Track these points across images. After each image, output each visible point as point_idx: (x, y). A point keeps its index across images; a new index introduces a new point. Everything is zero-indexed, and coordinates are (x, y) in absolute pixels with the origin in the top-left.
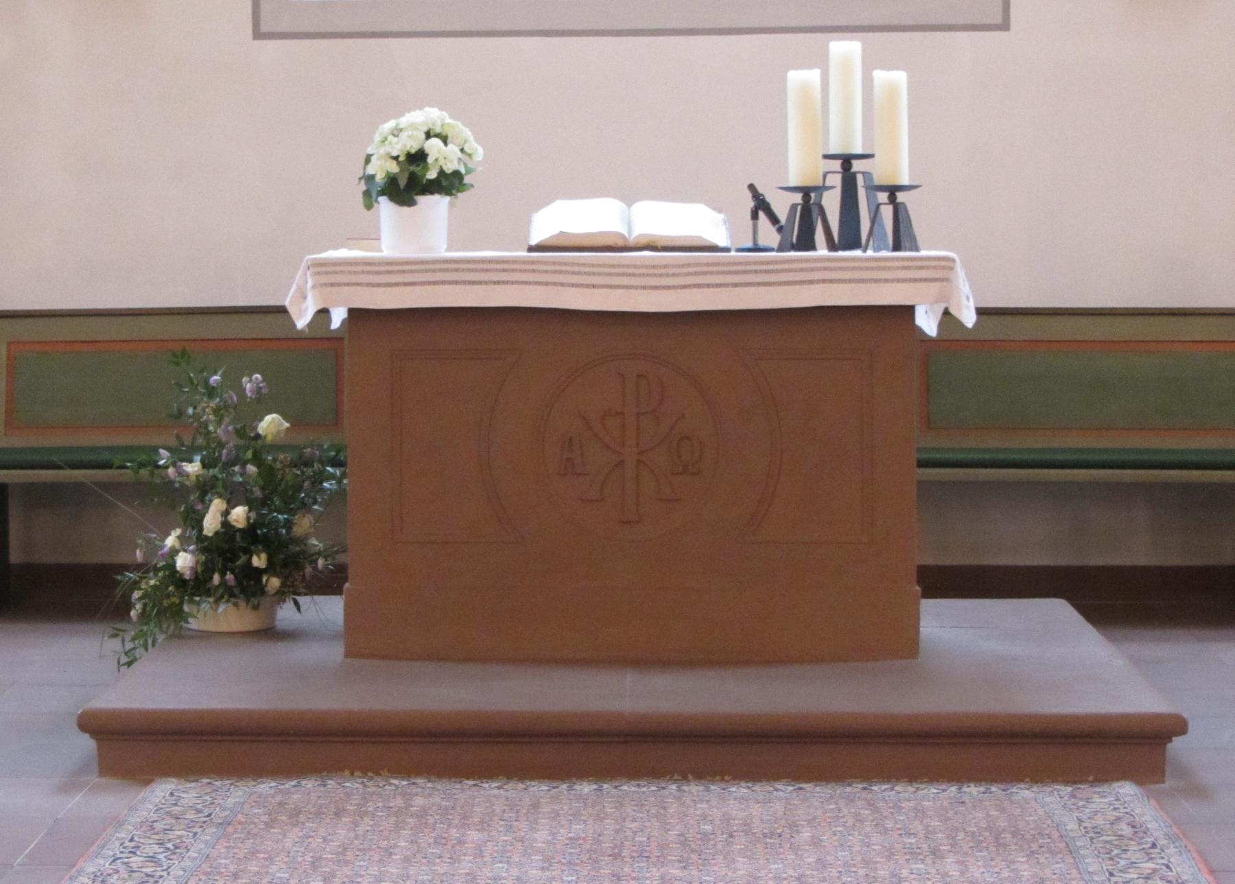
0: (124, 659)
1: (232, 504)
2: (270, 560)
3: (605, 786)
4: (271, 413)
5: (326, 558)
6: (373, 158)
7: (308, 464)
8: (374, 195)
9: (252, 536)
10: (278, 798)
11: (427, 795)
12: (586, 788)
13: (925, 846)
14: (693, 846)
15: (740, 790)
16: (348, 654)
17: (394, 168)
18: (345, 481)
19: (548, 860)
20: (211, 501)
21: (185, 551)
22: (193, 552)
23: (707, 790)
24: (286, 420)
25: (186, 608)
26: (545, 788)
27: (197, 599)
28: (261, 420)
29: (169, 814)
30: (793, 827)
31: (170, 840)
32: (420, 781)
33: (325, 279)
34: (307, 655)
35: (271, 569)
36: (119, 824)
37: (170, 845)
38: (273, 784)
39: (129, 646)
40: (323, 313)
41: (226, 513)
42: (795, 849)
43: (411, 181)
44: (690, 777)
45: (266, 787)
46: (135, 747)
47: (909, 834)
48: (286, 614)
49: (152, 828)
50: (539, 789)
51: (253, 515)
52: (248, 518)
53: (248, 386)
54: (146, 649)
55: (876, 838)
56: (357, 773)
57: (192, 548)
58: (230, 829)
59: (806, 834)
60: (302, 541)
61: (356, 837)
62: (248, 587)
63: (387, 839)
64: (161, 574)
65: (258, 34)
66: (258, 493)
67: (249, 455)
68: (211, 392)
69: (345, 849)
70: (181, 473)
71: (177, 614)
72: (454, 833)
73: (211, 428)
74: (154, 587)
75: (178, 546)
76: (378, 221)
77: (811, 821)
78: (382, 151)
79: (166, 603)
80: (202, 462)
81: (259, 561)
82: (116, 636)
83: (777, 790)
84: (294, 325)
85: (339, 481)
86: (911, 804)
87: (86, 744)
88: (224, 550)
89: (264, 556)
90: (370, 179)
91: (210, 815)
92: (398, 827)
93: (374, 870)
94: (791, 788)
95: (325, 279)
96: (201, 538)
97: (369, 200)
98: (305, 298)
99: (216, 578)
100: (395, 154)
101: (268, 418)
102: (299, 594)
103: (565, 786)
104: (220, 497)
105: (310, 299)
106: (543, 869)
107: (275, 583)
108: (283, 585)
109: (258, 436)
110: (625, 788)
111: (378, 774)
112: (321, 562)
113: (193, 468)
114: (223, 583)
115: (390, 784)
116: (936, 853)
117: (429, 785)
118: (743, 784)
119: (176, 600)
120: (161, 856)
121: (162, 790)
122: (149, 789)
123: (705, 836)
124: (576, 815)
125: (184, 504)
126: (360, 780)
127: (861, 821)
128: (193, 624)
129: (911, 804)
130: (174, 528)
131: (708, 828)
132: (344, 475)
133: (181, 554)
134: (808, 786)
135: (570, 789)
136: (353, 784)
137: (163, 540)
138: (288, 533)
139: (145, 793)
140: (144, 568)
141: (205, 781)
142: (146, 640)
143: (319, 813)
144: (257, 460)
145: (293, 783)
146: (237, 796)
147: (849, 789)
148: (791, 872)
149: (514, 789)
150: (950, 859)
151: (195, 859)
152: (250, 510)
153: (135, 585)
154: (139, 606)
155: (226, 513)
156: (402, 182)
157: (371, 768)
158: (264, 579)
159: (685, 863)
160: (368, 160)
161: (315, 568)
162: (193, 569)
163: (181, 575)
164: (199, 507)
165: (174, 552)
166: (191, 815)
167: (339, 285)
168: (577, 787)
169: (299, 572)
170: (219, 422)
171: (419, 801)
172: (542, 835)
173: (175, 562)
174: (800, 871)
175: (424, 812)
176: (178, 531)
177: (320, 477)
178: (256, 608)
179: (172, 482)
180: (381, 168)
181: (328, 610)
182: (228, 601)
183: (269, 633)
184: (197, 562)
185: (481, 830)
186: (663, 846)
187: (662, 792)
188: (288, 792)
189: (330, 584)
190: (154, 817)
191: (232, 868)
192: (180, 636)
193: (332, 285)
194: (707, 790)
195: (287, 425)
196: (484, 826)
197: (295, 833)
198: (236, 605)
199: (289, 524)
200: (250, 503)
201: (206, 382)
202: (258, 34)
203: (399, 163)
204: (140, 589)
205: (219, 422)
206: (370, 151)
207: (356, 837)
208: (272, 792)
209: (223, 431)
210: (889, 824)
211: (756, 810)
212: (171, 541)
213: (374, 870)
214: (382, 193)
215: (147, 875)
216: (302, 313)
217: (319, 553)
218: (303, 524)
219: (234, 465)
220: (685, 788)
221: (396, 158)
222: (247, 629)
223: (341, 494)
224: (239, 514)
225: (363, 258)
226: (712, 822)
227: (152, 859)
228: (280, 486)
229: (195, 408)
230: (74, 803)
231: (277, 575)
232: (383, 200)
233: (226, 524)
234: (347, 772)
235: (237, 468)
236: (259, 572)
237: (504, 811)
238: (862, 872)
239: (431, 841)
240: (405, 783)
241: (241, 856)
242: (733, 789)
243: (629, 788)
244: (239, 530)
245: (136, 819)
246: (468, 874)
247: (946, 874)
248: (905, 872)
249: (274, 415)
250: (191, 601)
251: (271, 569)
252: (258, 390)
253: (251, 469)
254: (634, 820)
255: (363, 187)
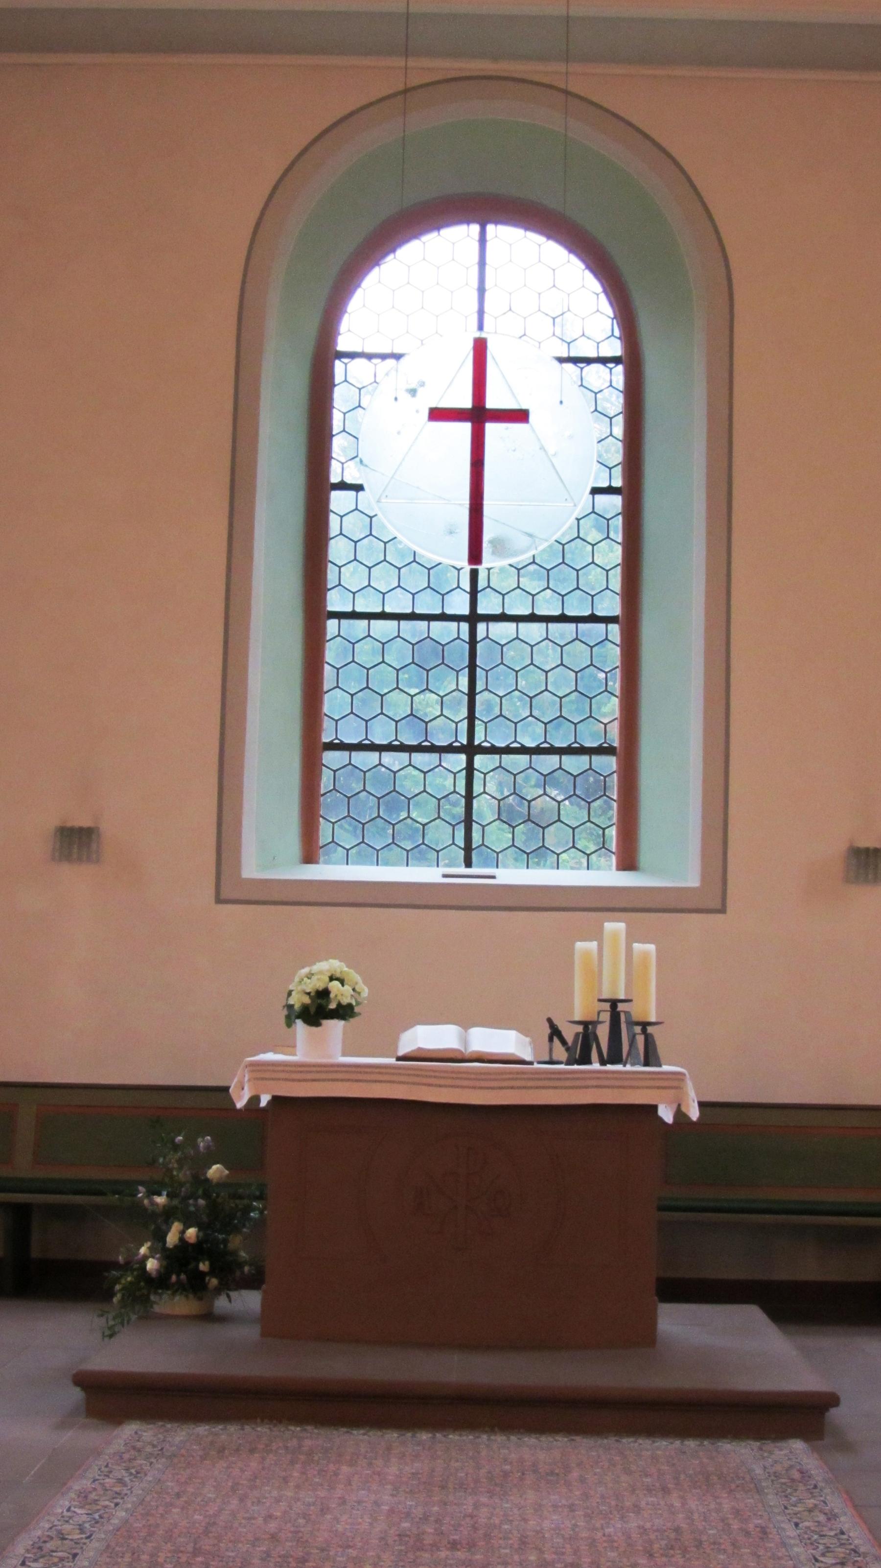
0: (107, 1332)
1: (187, 1227)
2: (211, 1265)
3: (438, 1435)
4: (218, 1163)
5: (250, 1265)
6: (293, 993)
7: (241, 1197)
8: (293, 1017)
9: (199, 1249)
10: (210, 1438)
11: (314, 1438)
12: (424, 1436)
13: (658, 1485)
14: (497, 1481)
15: (531, 1440)
16: (263, 1335)
17: (307, 1000)
18: (266, 1212)
19: (396, 1489)
20: (173, 1223)
21: (153, 1257)
22: (158, 1259)
23: (509, 1439)
24: (227, 1169)
25: (152, 1298)
26: (396, 1435)
27: (160, 1291)
28: (210, 1168)
29: (134, 1448)
30: (567, 1469)
31: (133, 1467)
32: (309, 1428)
33: (259, 1075)
34: (234, 1335)
35: (212, 1272)
36: (97, 1453)
37: (133, 1471)
38: (207, 1427)
39: (111, 1323)
40: (255, 1099)
41: (183, 1232)
42: (568, 1484)
43: (318, 1010)
44: (496, 1429)
45: (202, 1429)
46: (112, 1398)
47: (646, 1476)
48: (221, 1304)
49: (121, 1458)
50: (392, 1435)
51: (201, 1234)
52: (198, 1237)
53: (202, 1145)
54: (123, 1326)
55: (624, 1478)
56: (266, 1421)
57: (158, 1256)
58: (176, 1460)
59: (575, 1474)
60: (234, 1253)
61: (263, 1469)
62: (196, 1285)
63: (285, 1470)
64: (135, 1273)
65: (219, 900)
66: (205, 1219)
67: (200, 1192)
68: (176, 1147)
69: (256, 1478)
70: (153, 1203)
71: (145, 1301)
72: (332, 1467)
73: (175, 1173)
74: (131, 1283)
75: (148, 1253)
76: (295, 1034)
77: (580, 1464)
78: (300, 988)
79: (138, 1294)
80: (168, 1195)
81: (204, 1266)
82: (102, 1315)
83: (556, 1441)
84: (234, 1104)
85: (261, 1212)
86: (649, 1453)
87: (77, 1394)
88: (180, 1258)
89: (207, 1263)
90: (290, 1007)
91: (162, 1449)
92: (292, 1462)
93: (275, 1493)
94: (566, 1439)
95: (259, 1075)
96: (164, 1249)
97: (289, 1023)
98: (243, 1089)
99: (174, 1278)
100: (308, 991)
101: (215, 1167)
102: (230, 1290)
103: (409, 1435)
104: (179, 1220)
105: (246, 1088)
106: (392, 1495)
107: (214, 1282)
108: (220, 1283)
109: (207, 1180)
110: (451, 1436)
111: (280, 1422)
112: (246, 1269)
113: (161, 1200)
114: (179, 1281)
115: (288, 1430)
116: (665, 1490)
117: (316, 1431)
118: (534, 1436)
119: (145, 1292)
120: (127, 1479)
121: (129, 1429)
122: (120, 1428)
123: (506, 1475)
124: (417, 1456)
125: (155, 1224)
126: (267, 1426)
127: (614, 1465)
128: (157, 1309)
129: (649, 1453)
130: (146, 1241)
131: (508, 1467)
132: (265, 1208)
133: (150, 1259)
134: (578, 1439)
135: (413, 1436)
136: (263, 1429)
137: (139, 1249)
138: (225, 1246)
139: (117, 1431)
140: (127, 1266)
141: (160, 1423)
142: (123, 1319)
143: (238, 1450)
144: (206, 1195)
145: (220, 1427)
146: (181, 1435)
147: (605, 1441)
148: (564, 1502)
149: (374, 1435)
150: (675, 1495)
151: (150, 1481)
152: (199, 1230)
153: (117, 1280)
154: (119, 1296)
155: (183, 1232)
156: (313, 1010)
157: (276, 1418)
158: (207, 1278)
159: (491, 1494)
160: (290, 994)
161: (243, 1272)
162: (158, 1271)
163: (150, 1274)
164: (164, 1227)
165: (145, 1258)
166: (149, 1449)
167: (266, 1079)
168: (418, 1435)
169: (231, 1275)
170: (180, 1168)
171: (308, 1443)
172: (393, 1470)
173: (145, 1266)
174: (570, 1502)
175: (310, 1453)
176: (149, 1244)
177: (249, 1209)
178: (200, 1299)
179: (146, 1210)
180: (298, 1000)
181: (250, 1301)
182: (181, 1293)
183: (209, 1317)
184: (161, 1266)
185: (351, 1465)
186: (477, 1481)
187: (477, 1441)
188: (216, 1434)
189: (253, 1282)
190: (123, 1449)
191: (176, 1490)
192: (148, 1317)
193: (262, 1079)
194: (509, 1439)
195: (227, 1172)
196: (352, 1463)
197: (222, 1464)
198: (187, 1296)
199: (225, 1242)
200: (201, 1227)
201: (173, 1141)
202: (219, 900)
203: (311, 997)
204: (120, 1283)
205: (180, 1168)
206: (291, 987)
207: (263, 1469)
208: (206, 1433)
209: (183, 1175)
210: (633, 1467)
211: (542, 1456)
212: (143, 1250)
213: (275, 1493)
214: (298, 1017)
215: (116, 1493)
216: (240, 1098)
217: (246, 1263)
218: (235, 1242)
219: (189, 1198)
220: (492, 1437)
221: (309, 994)
222: (194, 1313)
223: (261, 1223)
224: (192, 1232)
225: (283, 1062)
226: (511, 1463)
227: (120, 1481)
228: (220, 1214)
229: (165, 1158)
230: (67, 1437)
231: (216, 1277)
232: (299, 1023)
233: (182, 1240)
234: (259, 1420)
235: (191, 1201)
236: (203, 1274)
237: (367, 1452)
238: (613, 1503)
239: (316, 1473)
240: (298, 1429)
241: (183, 1480)
242: (526, 1439)
243: (453, 1437)
244: (192, 1245)
245: (111, 1450)
246: (340, 1498)
247: (672, 1505)
248: (643, 1504)
249: (218, 1166)
250: (156, 1293)
251: (212, 1272)
252: (208, 1148)
253: (201, 1202)
254: (457, 1461)
255: (285, 1012)
